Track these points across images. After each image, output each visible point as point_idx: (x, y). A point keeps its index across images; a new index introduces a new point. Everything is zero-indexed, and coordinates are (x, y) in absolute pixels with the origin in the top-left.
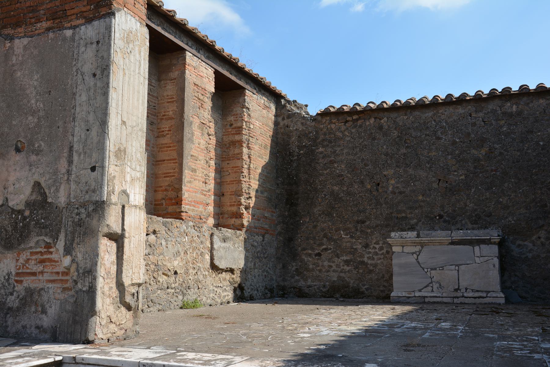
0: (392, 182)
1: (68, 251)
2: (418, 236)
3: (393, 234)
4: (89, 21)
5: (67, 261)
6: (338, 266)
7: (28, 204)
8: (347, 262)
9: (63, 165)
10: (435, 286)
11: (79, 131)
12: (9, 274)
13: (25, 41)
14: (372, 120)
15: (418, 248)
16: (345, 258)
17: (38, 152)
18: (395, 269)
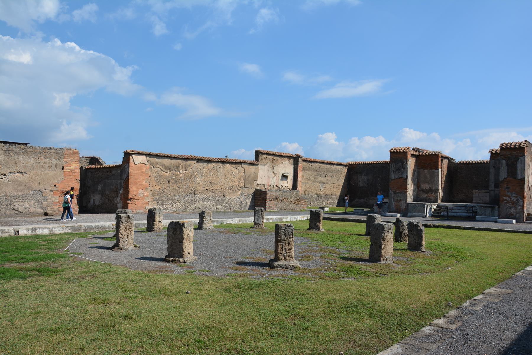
0: (474, 179)
1: (434, 194)
2: (479, 191)
3: (474, 190)
4: (436, 170)
5: (435, 195)
6: (462, 196)
7: (429, 189)
8: (464, 195)
9: (433, 185)
10: (482, 200)
11: (435, 182)
12: (427, 196)
13: (427, 171)
14: (471, 165)
15: (478, 193)
16: (464, 194)
17: (430, 183)
18: (474, 197)
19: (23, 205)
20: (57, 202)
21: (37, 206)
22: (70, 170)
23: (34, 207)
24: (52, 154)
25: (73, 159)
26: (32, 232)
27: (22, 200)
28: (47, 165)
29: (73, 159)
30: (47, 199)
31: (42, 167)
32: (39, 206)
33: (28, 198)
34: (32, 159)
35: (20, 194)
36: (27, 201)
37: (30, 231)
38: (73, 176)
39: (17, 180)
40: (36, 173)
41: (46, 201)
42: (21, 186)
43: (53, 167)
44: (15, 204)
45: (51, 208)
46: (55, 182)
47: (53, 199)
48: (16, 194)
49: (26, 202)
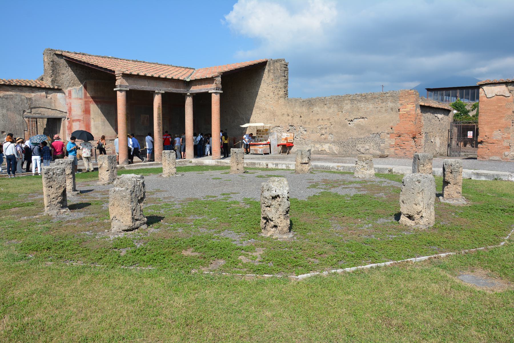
19: (364, 147)
20: (393, 145)
21: (376, 148)
22: (405, 112)
23: (373, 149)
24: (388, 97)
25: (408, 100)
26: (275, 166)
27: (364, 142)
28: (384, 109)
29: (408, 100)
30: (384, 142)
31: (379, 111)
32: (377, 148)
33: (368, 141)
34: (371, 105)
35: (362, 137)
36: (368, 143)
37: (275, 165)
38: (409, 118)
39: (360, 125)
40: (374, 117)
41: (384, 144)
42: (363, 129)
43: (390, 110)
44: (359, 145)
45: (388, 150)
46: (391, 125)
47: (390, 141)
48: (359, 136)
49: (367, 144)
